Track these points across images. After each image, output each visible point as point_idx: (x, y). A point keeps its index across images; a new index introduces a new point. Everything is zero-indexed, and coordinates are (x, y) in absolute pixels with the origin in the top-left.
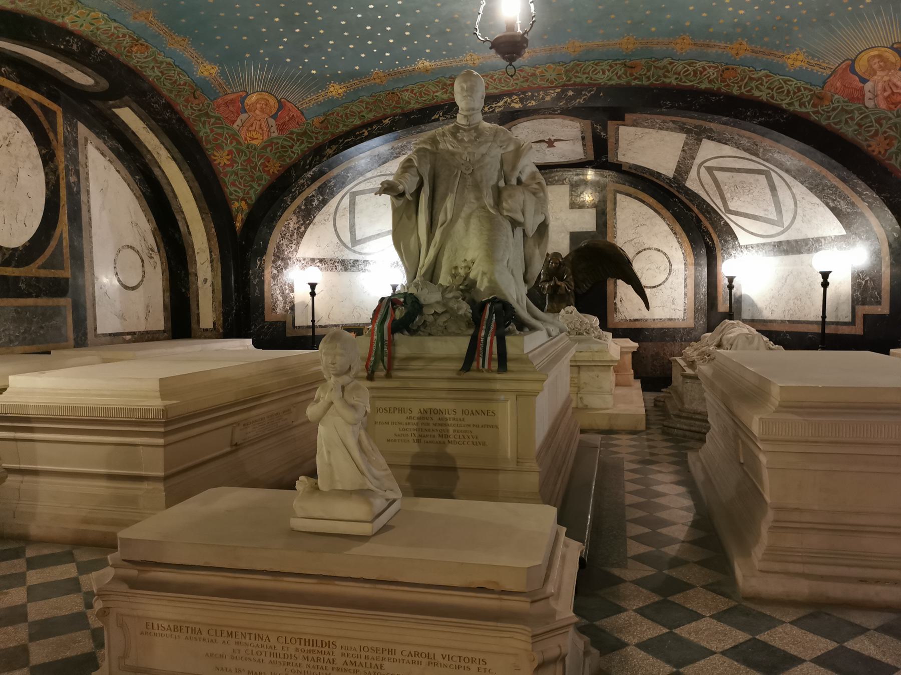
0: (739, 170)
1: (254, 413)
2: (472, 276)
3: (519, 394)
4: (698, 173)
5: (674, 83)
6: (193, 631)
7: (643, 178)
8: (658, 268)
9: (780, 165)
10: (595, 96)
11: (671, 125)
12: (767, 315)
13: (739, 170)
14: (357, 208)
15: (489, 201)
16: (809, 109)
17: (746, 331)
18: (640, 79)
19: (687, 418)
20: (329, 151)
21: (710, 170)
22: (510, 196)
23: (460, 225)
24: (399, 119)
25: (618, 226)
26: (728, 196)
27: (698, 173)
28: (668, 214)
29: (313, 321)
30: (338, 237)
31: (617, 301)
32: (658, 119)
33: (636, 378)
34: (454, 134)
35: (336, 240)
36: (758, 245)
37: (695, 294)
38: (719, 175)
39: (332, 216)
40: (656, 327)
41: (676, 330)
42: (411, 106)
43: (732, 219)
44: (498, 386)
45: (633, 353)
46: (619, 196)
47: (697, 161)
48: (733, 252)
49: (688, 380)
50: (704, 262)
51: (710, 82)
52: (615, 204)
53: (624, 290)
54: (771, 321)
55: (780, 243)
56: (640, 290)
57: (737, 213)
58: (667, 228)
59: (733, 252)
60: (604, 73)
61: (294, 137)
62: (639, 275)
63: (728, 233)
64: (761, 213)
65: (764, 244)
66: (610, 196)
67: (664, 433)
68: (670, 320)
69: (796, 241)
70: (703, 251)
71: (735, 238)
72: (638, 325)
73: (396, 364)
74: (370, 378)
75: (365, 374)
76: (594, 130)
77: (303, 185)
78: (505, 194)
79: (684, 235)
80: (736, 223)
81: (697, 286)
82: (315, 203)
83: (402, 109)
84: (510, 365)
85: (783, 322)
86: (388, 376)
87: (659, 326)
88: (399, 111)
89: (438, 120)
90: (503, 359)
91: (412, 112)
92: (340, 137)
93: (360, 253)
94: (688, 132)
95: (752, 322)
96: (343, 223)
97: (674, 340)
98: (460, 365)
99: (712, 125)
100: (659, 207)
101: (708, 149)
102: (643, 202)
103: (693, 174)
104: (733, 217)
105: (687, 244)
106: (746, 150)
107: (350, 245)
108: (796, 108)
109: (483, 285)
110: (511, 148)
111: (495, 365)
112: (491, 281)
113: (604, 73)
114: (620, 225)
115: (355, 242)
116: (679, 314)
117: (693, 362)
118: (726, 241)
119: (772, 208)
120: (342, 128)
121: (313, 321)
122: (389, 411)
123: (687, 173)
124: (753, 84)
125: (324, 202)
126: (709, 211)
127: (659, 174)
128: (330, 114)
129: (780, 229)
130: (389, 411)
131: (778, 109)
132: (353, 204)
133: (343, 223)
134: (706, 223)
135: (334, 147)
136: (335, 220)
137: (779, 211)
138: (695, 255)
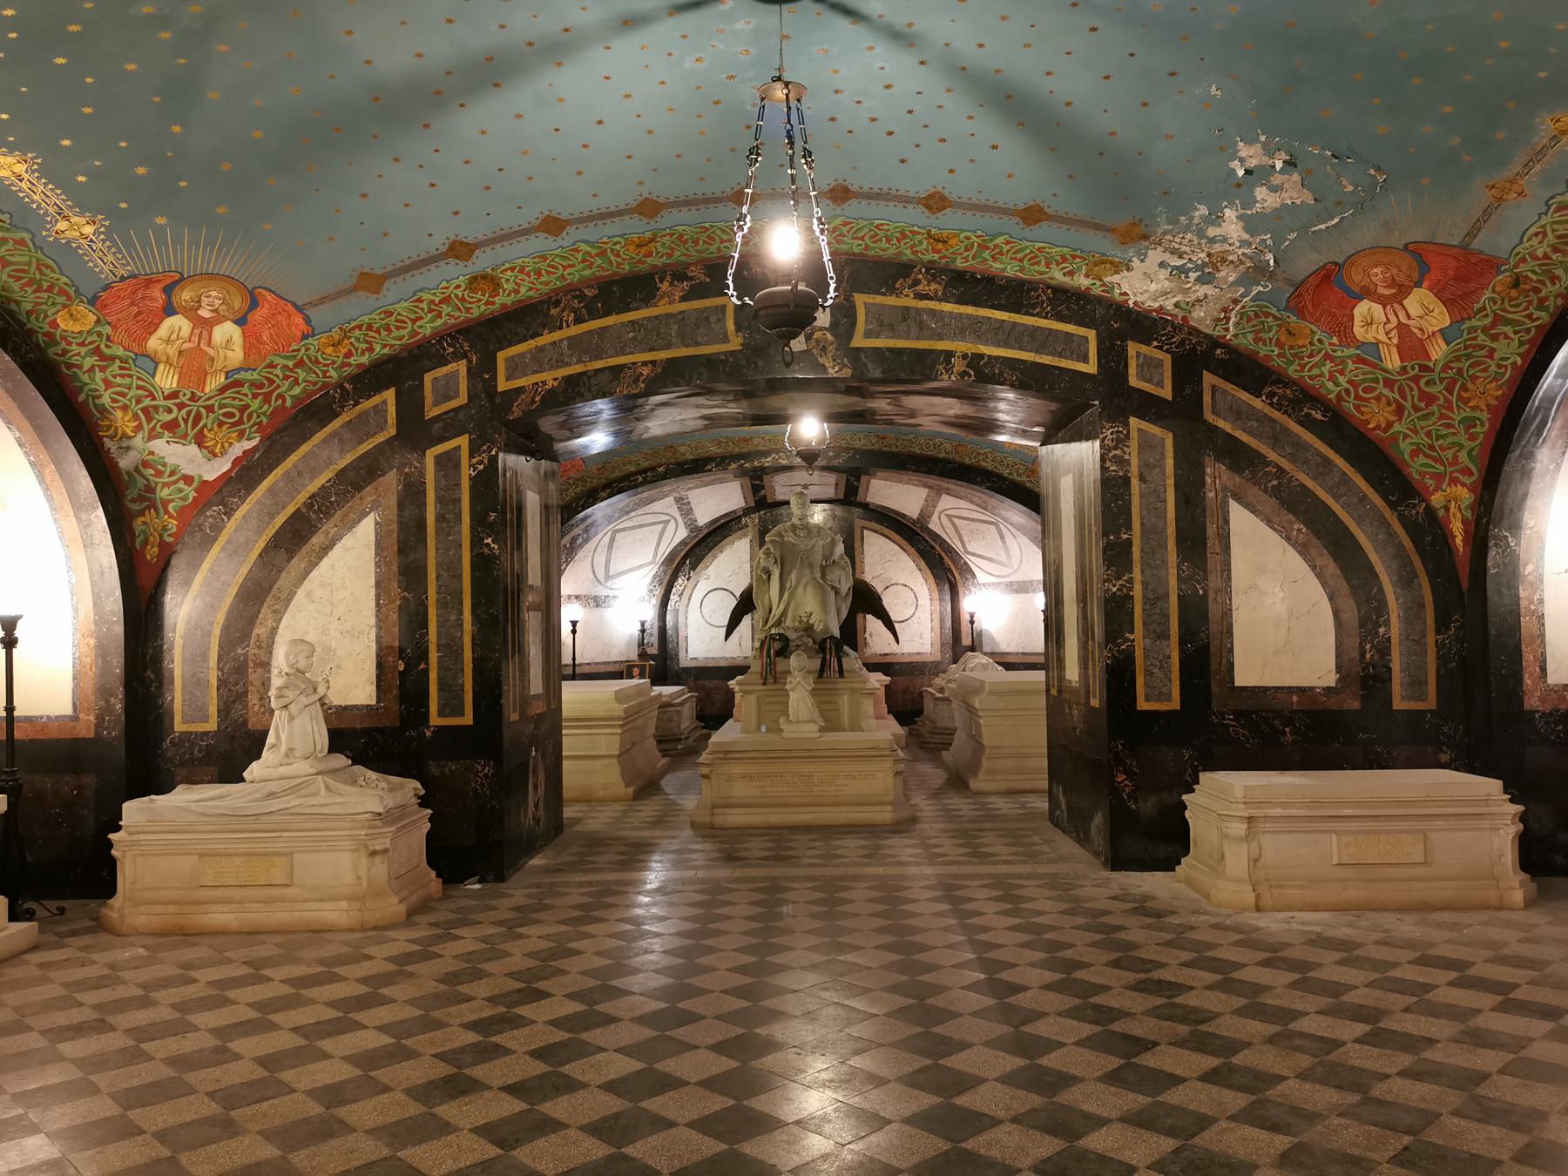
0: (973, 520)
1: (639, 721)
2: (811, 622)
3: (853, 690)
4: (939, 518)
5: (918, 451)
6: (751, 777)
7: (883, 514)
8: (906, 603)
9: (1005, 519)
10: (852, 458)
11: (916, 482)
12: (1004, 648)
13: (973, 520)
14: (615, 544)
15: (818, 575)
16: (1024, 479)
17: (984, 661)
18: (890, 447)
19: (938, 734)
20: (603, 494)
21: (949, 516)
22: (831, 572)
23: (801, 589)
24: (673, 469)
25: (865, 561)
26: (965, 539)
27: (939, 518)
28: (913, 551)
29: (574, 659)
30: (594, 573)
31: (867, 635)
32: (905, 478)
33: (889, 713)
34: (794, 531)
35: (592, 576)
36: (993, 584)
37: (941, 628)
38: (957, 521)
39: (591, 554)
40: (905, 661)
41: (925, 664)
42: (685, 457)
43: (971, 561)
44: (840, 686)
45: (886, 686)
46: (865, 532)
47: (939, 509)
48: (973, 589)
49: (940, 702)
50: (948, 597)
51: (946, 453)
52: (862, 539)
53: (873, 624)
54: (1008, 654)
55: (1011, 582)
56: (889, 624)
57: (974, 555)
58: (912, 564)
59: (973, 589)
60: (860, 440)
61: (571, 482)
62: (888, 610)
63: (967, 571)
64: (994, 557)
65: (998, 583)
66: (857, 533)
67: (921, 748)
68: (918, 654)
69: (1024, 582)
70: (947, 587)
71: (974, 576)
72: (888, 659)
73: (778, 676)
74: (764, 684)
75: (761, 681)
76: (848, 480)
77: (573, 525)
78: (828, 571)
79: (928, 571)
80: (973, 562)
81: (942, 620)
82: (580, 540)
83: (677, 458)
84: (845, 674)
85: (1017, 654)
86: (775, 682)
87: (908, 660)
88: (674, 460)
89: (710, 470)
90: (841, 672)
91: (686, 462)
92: (614, 481)
93: (611, 589)
94: (930, 488)
95: (992, 655)
96: (600, 559)
97: (922, 673)
98: (817, 675)
99: (950, 486)
100: (904, 543)
101: (946, 502)
102: (889, 539)
103: (935, 517)
104: (969, 557)
105: (931, 580)
106: (978, 506)
107: (602, 581)
108: (1015, 476)
109: (818, 627)
110: (829, 540)
111: (837, 675)
112: (825, 625)
113: (860, 440)
114: (867, 561)
115: (608, 577)
116: (927, 649)
117: (942, 688)
118: (967, 579)
119: (1002, 552)
120: (617, 474)
121: (574, 659)
122: (774, 703)
123: (930, 517)
124: (981, 457)
125: (586, 541)
126: (950, 550)
127: (904, 516)
128: (353, 328)
129: (1011, 571)
130: (774, 703)
131: (1001, 477)
132: (612, 540)
133: (600, 559)
134: (947, 561)
135: (608, 491)
136: (593, 555)
137: (1009, 556)
138: (939, 591)
